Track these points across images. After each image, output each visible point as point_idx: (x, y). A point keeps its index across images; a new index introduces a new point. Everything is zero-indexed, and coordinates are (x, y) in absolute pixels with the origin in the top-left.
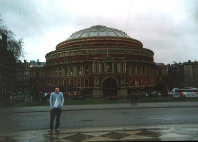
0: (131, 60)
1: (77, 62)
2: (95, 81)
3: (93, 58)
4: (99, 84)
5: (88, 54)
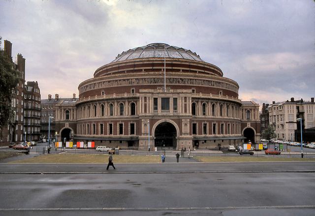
2: (143, 125)
5: (135, 84)
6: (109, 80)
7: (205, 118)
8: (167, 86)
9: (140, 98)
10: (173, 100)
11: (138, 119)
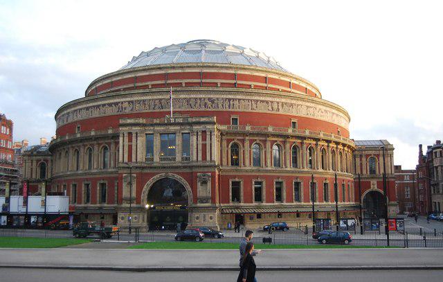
0: (248, 128)
1: (99, 133)
2: (124, 185)
3: (121, 121)
4: (134, 195)
5: (127, 111)
6: (88, 105)
7: (259, 171)
8: (174, 112)
9: (121, 135)
10: (181, 139)
11: (117, 175)
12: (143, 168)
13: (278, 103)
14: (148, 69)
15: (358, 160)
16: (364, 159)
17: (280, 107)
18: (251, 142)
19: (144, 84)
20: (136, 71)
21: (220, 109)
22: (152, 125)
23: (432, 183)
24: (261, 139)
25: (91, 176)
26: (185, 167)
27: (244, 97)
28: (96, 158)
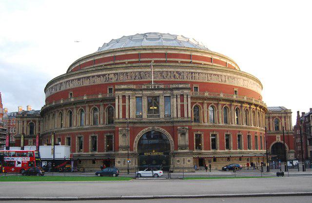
0: (206, 94)
1: (90, 98)
2: (120, 136)
3: (116, 87)
5: (113, 81)
6: (79, 77)
12: (135, 123)
13: (225, 76)
14: (125, 50)
15: (267, 120)
16: (271, 120)
17: (227, 80)
18: (208, 104)
19: (121, 61)
20: (116, 51)
21: (185, 80)
22: (141, 90)
23: (309, 137)
24: (215, 102)
25: (83, 131)
26: (168, 122)
27: (202, 71)
28: (87, 117)
